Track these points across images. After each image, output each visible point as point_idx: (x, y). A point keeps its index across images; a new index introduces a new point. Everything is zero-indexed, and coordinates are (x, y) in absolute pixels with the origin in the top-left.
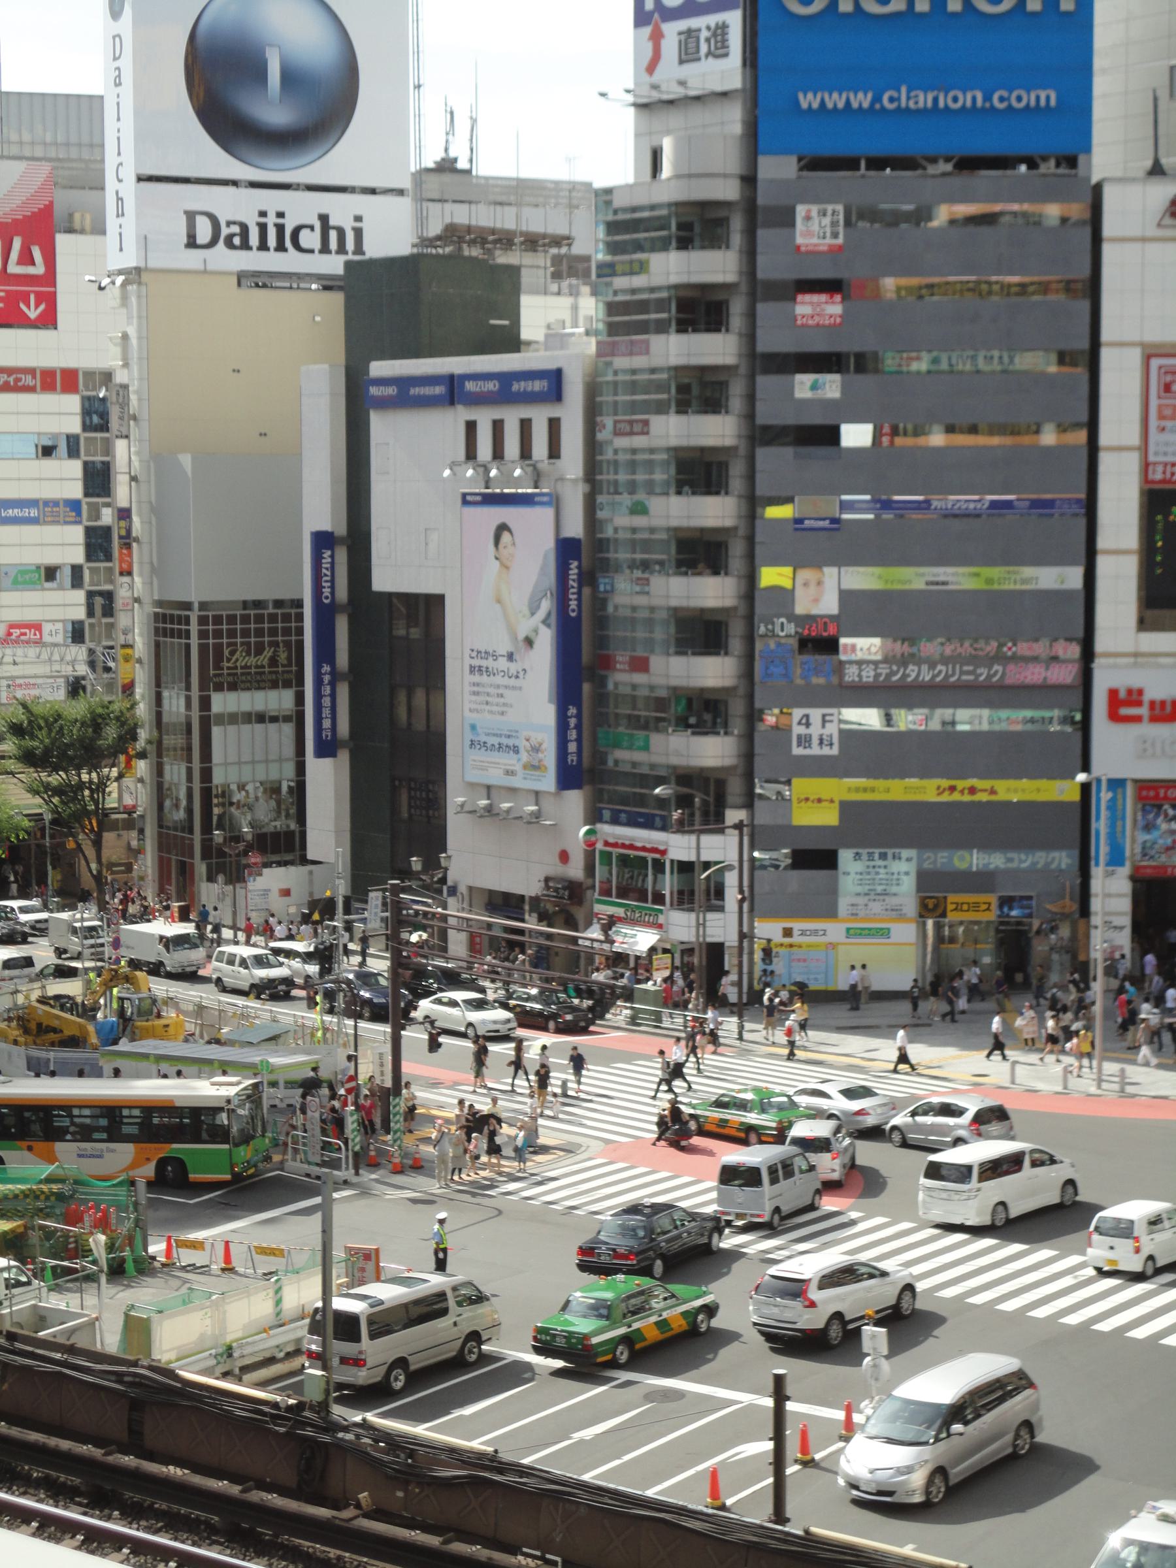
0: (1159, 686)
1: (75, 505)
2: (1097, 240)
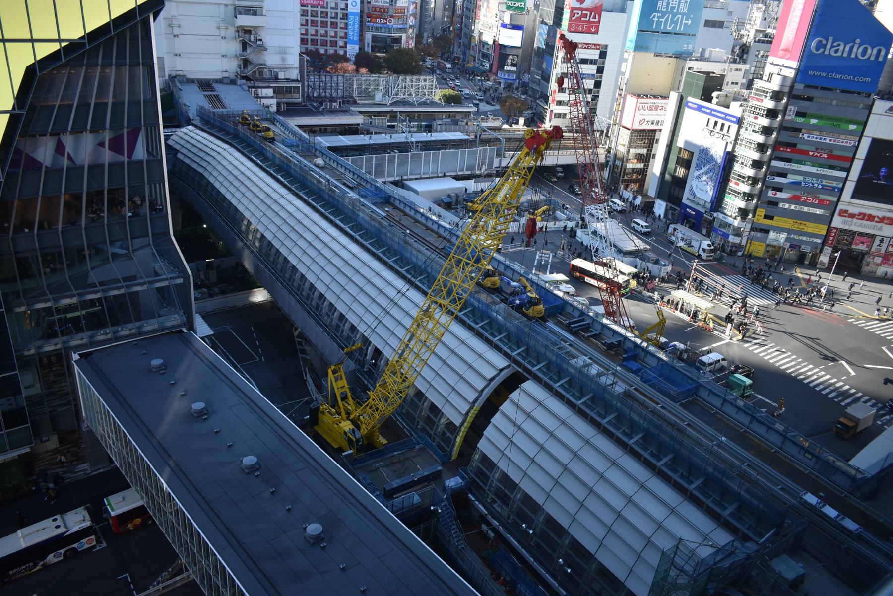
0: (852, 210)
1: (593, 75)
2: (870, 113)
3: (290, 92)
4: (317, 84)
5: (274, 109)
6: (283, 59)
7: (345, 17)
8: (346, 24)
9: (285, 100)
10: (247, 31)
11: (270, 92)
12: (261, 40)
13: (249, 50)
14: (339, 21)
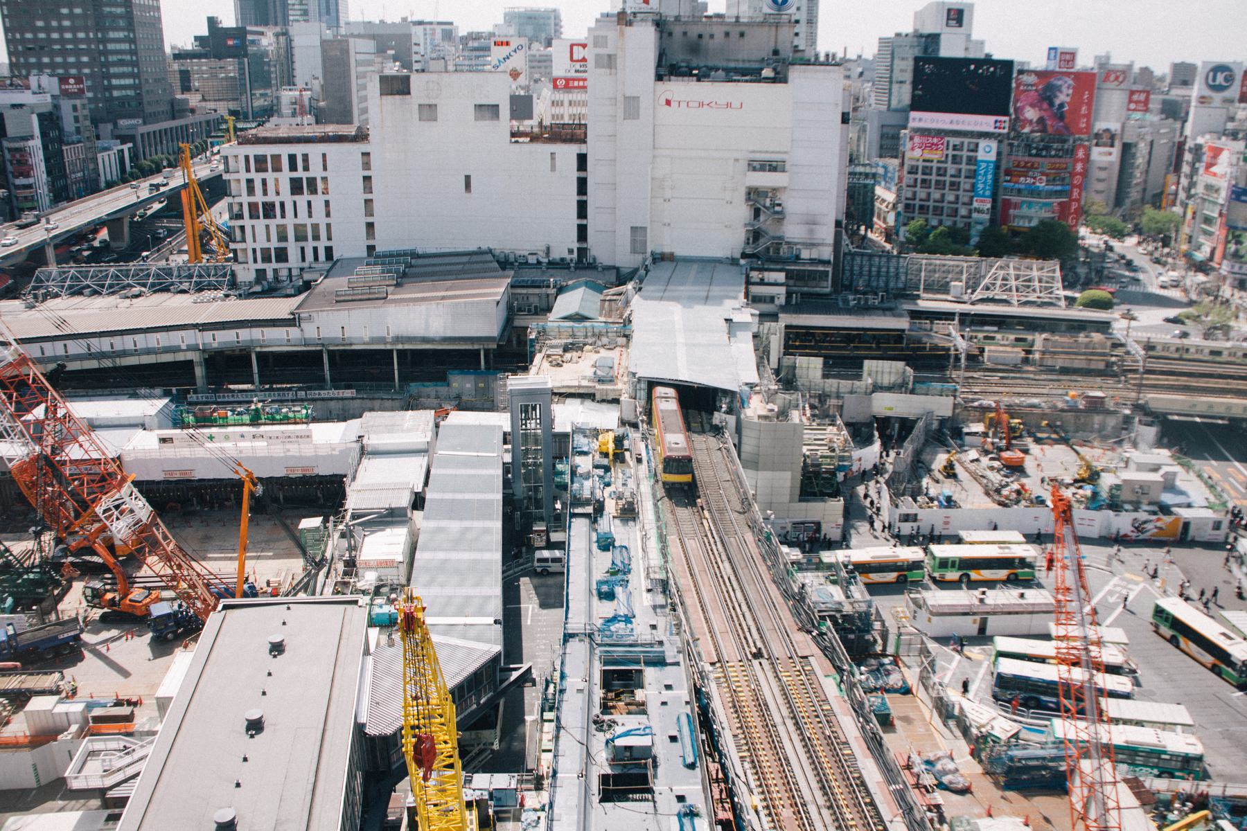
3: (815, 279)
4: (884, 269)
5: (782, 300)
6: (811, 231)
7: (972, 175)
8: (973, 185)
9: (805, 289)
10: (754, 195)
11: (780, 277)
12: (779, 205)
13: (762, 218)
14: (962, 179)
